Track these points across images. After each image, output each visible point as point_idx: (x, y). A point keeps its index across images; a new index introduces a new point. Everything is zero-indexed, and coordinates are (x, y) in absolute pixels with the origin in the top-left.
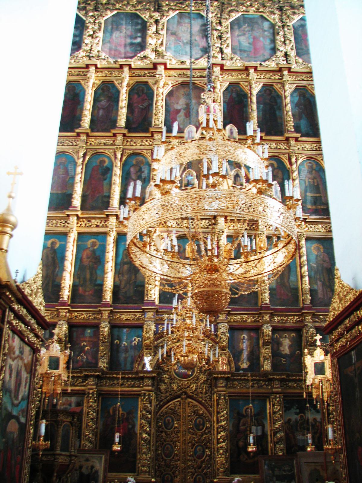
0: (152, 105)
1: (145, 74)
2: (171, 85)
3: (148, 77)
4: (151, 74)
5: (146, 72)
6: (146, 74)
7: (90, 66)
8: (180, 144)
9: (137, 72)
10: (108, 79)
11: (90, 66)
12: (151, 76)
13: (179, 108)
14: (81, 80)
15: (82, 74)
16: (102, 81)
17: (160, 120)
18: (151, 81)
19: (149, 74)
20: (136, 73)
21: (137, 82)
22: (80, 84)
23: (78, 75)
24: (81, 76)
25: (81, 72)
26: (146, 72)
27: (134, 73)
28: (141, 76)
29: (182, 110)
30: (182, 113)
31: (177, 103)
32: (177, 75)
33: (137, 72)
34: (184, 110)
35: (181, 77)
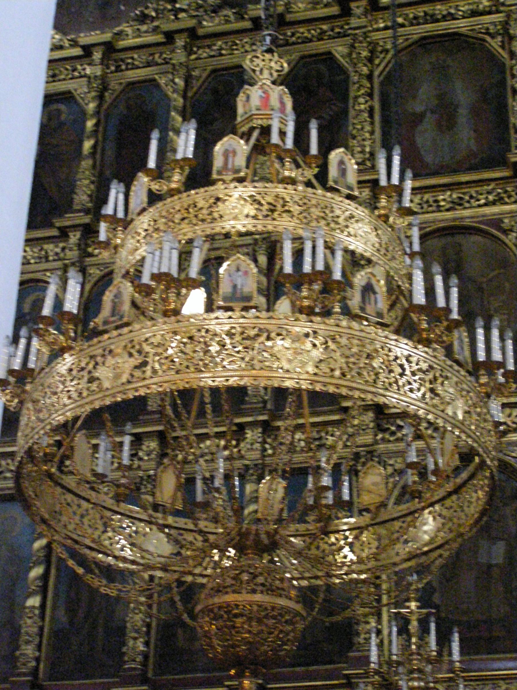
0: (345, 112)
1: (323, 32)
2: (392, 52)
3: (330, 38)
4: (337, 30)
5: (325, 27)
6: (325, 32)
7: (176, 36)
8: (425, 206)
9: (301, 30)
10: (227, 61)
11: (176, 36)
12: (339, 35)
13: (419, 108)
14: (156, 77)
15: (160, 61)
16: (209, 68)
17: (368, 149)
18: (340, 49)
19: (332, 30)
20: (298, 35)
21: (302, 57)
22: (158, 86)
23: (148, 65)
24: (157, 64)
25: (157, 56)
26: (325, 27)
27: (293, 35)
28: (311, 41)
29: (428, 115)
30: (429, 121)
31: (414, 97)
32: (406, 23)
33: (301, 30)
34: (433, 112)
35: (419, 24)
